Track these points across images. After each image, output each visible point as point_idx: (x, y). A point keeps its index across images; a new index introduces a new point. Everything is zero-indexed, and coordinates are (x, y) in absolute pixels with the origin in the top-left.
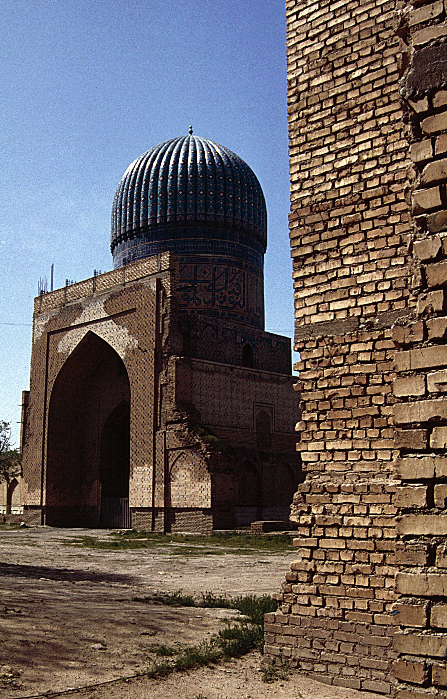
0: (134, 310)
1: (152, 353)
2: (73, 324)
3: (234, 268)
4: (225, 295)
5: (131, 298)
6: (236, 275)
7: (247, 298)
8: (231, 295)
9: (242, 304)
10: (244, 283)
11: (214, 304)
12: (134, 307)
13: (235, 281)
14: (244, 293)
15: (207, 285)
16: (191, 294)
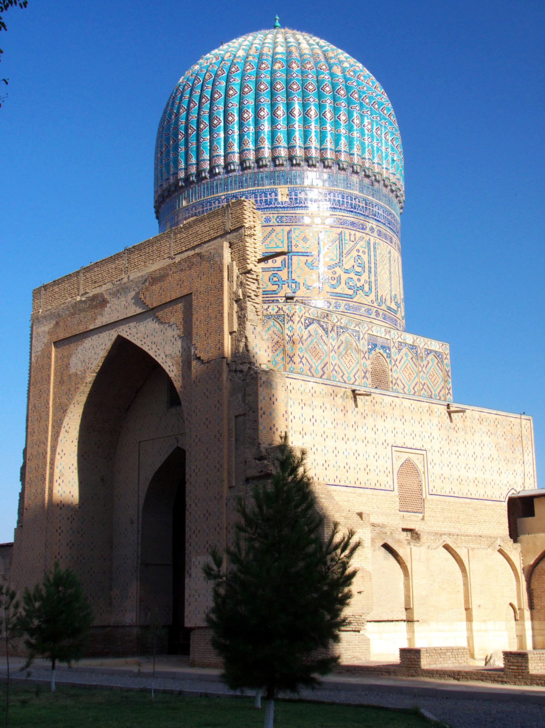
2: (91, 327)
3: (353, 232)
4: (340, 276)
6: (356, 244)
7: (376, 281)
8: (348, 275)
10: (369, 255)
13: (354, 253)
14: (370, 272)
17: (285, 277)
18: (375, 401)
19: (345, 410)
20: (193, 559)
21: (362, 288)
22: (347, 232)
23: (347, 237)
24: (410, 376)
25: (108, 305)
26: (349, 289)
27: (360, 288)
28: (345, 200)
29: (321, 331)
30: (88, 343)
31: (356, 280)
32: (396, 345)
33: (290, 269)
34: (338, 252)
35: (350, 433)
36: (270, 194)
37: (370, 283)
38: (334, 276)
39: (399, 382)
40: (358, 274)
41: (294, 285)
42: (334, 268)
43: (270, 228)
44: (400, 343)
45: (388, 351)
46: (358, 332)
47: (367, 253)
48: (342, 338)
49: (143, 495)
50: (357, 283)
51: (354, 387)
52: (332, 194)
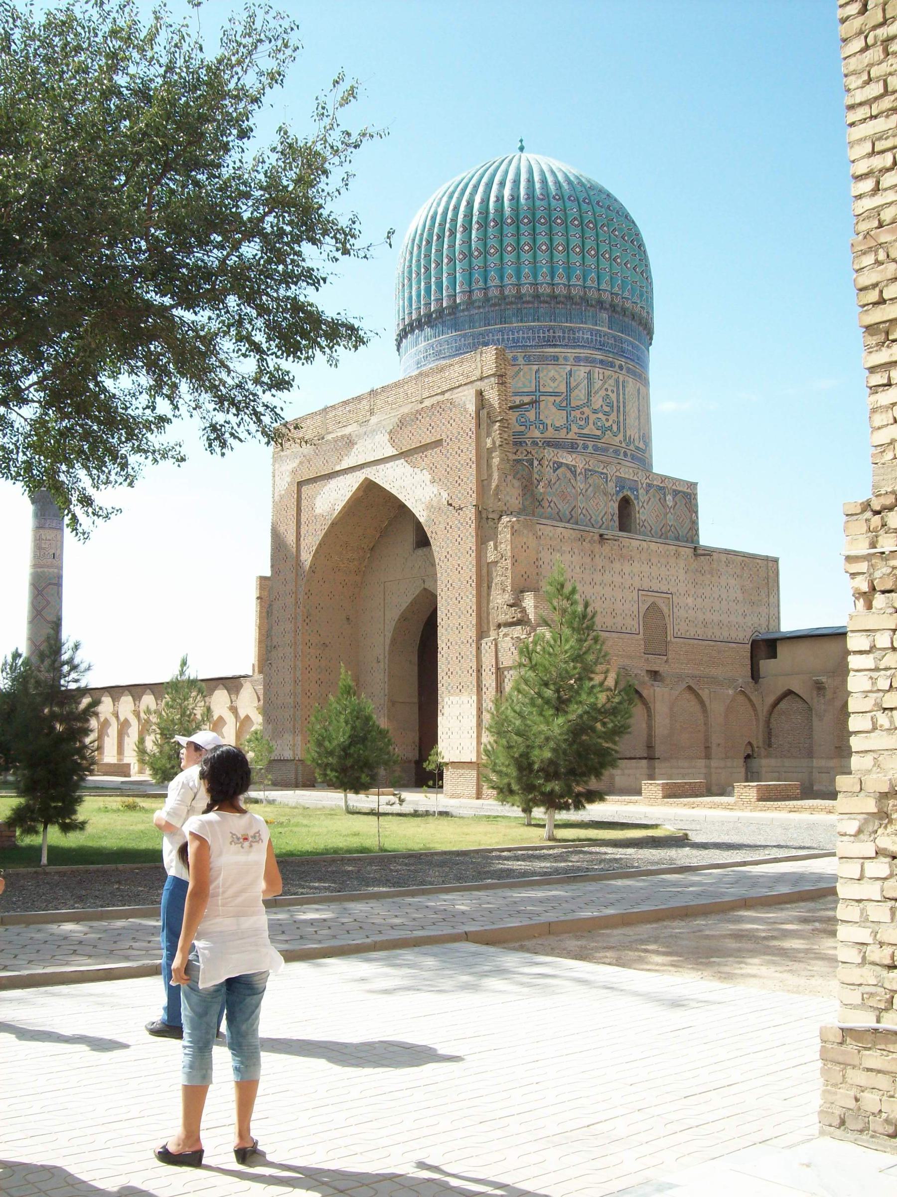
0: (438, 443)
1: (470, 513)
2: (338, 468)
3: (601, 371)
4: (588, 417)
5: (433, 424)
6: (605, 382)
9: (615, 428)
10: (618, 395)
11: (569, 430)
12: (439, 438)
14: (618, 411)
15: (558, 399)
16: (531, 415)
17: (532, 418)
19: (592, 555)
20: (446, 699)
21: (610, 428)
25: (356, 447)
28: (594, 338)
29: (569, 475)
30: (333, 483)
31: (604, 420)
32: (644, 485)
35: (598, 577)
37: (618, 422)
39: (646, 524)
40: (606, 414)
41: (541, 426)
44: (649, 485)
46: (606, 474)
48: (590, 481)
49: (389, 635)
51: (602, 531)
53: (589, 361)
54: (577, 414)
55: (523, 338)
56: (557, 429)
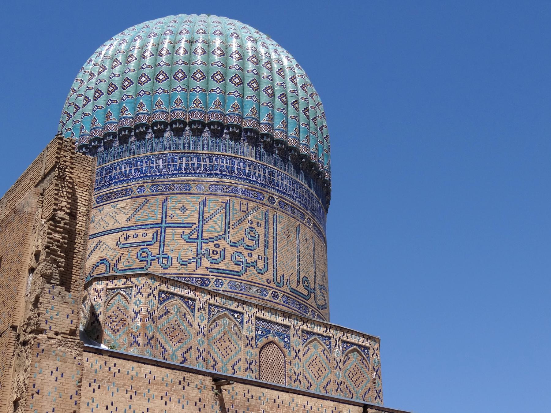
3: (245, 202)
6: (249, 214)
9: (260, 264)
10: (267, 229)
11: (198, 265)
14: (266, 247)
15: (187, 231)
16: (154, 249)
18: (250, 394)
21: (254, 265)
22: (237, 201)
23: (237, 207)
24: (319, 372)
26: (236, 264)
27: (251, 264)
29: (184, 308)
33: (162, 244)
34: (224, 222)
36: (146, 162)
37: (266, 260)
38: (216, 249)
39: (301, 378)
41: (165, 261)
42: (217, 240)
43: (143, 199)
45: (286, 339)
47: (263, 226)
50: (247, 258)
52: (220, 160)
53: (228, 189)
54: (211, 246)
55: (152, 167)
56: (184, 263)
